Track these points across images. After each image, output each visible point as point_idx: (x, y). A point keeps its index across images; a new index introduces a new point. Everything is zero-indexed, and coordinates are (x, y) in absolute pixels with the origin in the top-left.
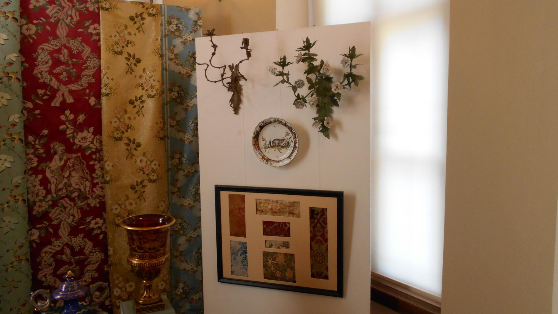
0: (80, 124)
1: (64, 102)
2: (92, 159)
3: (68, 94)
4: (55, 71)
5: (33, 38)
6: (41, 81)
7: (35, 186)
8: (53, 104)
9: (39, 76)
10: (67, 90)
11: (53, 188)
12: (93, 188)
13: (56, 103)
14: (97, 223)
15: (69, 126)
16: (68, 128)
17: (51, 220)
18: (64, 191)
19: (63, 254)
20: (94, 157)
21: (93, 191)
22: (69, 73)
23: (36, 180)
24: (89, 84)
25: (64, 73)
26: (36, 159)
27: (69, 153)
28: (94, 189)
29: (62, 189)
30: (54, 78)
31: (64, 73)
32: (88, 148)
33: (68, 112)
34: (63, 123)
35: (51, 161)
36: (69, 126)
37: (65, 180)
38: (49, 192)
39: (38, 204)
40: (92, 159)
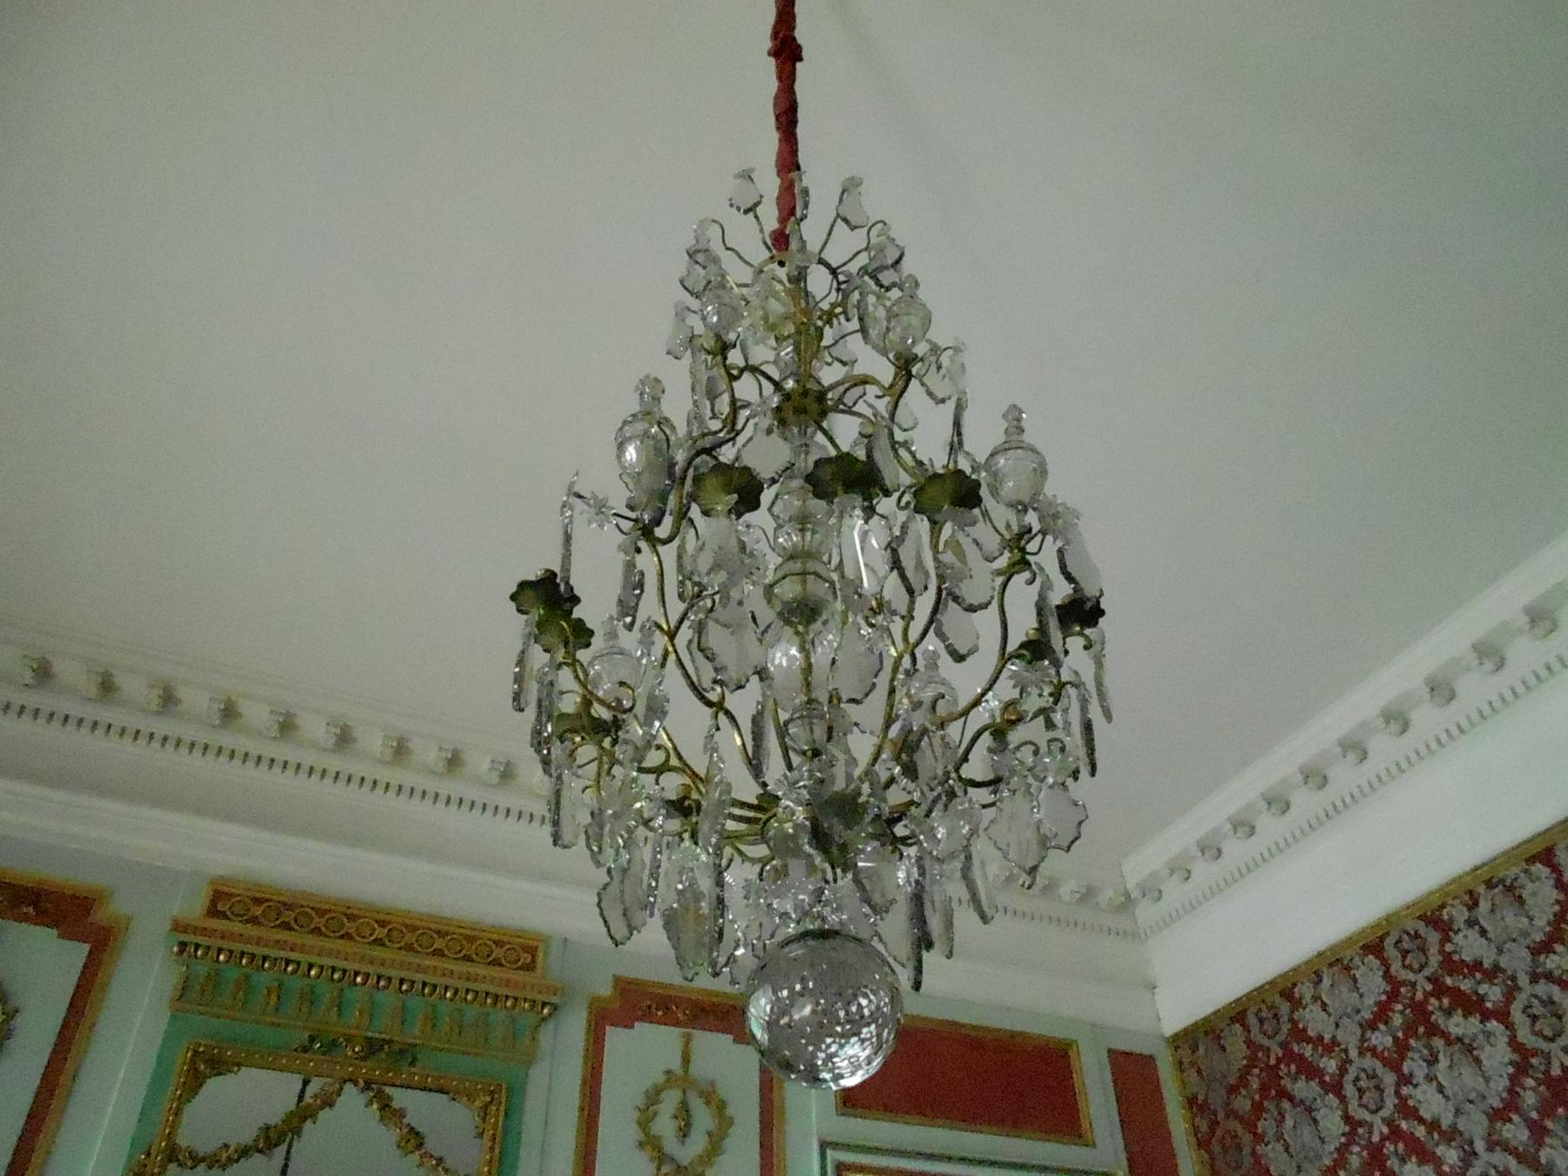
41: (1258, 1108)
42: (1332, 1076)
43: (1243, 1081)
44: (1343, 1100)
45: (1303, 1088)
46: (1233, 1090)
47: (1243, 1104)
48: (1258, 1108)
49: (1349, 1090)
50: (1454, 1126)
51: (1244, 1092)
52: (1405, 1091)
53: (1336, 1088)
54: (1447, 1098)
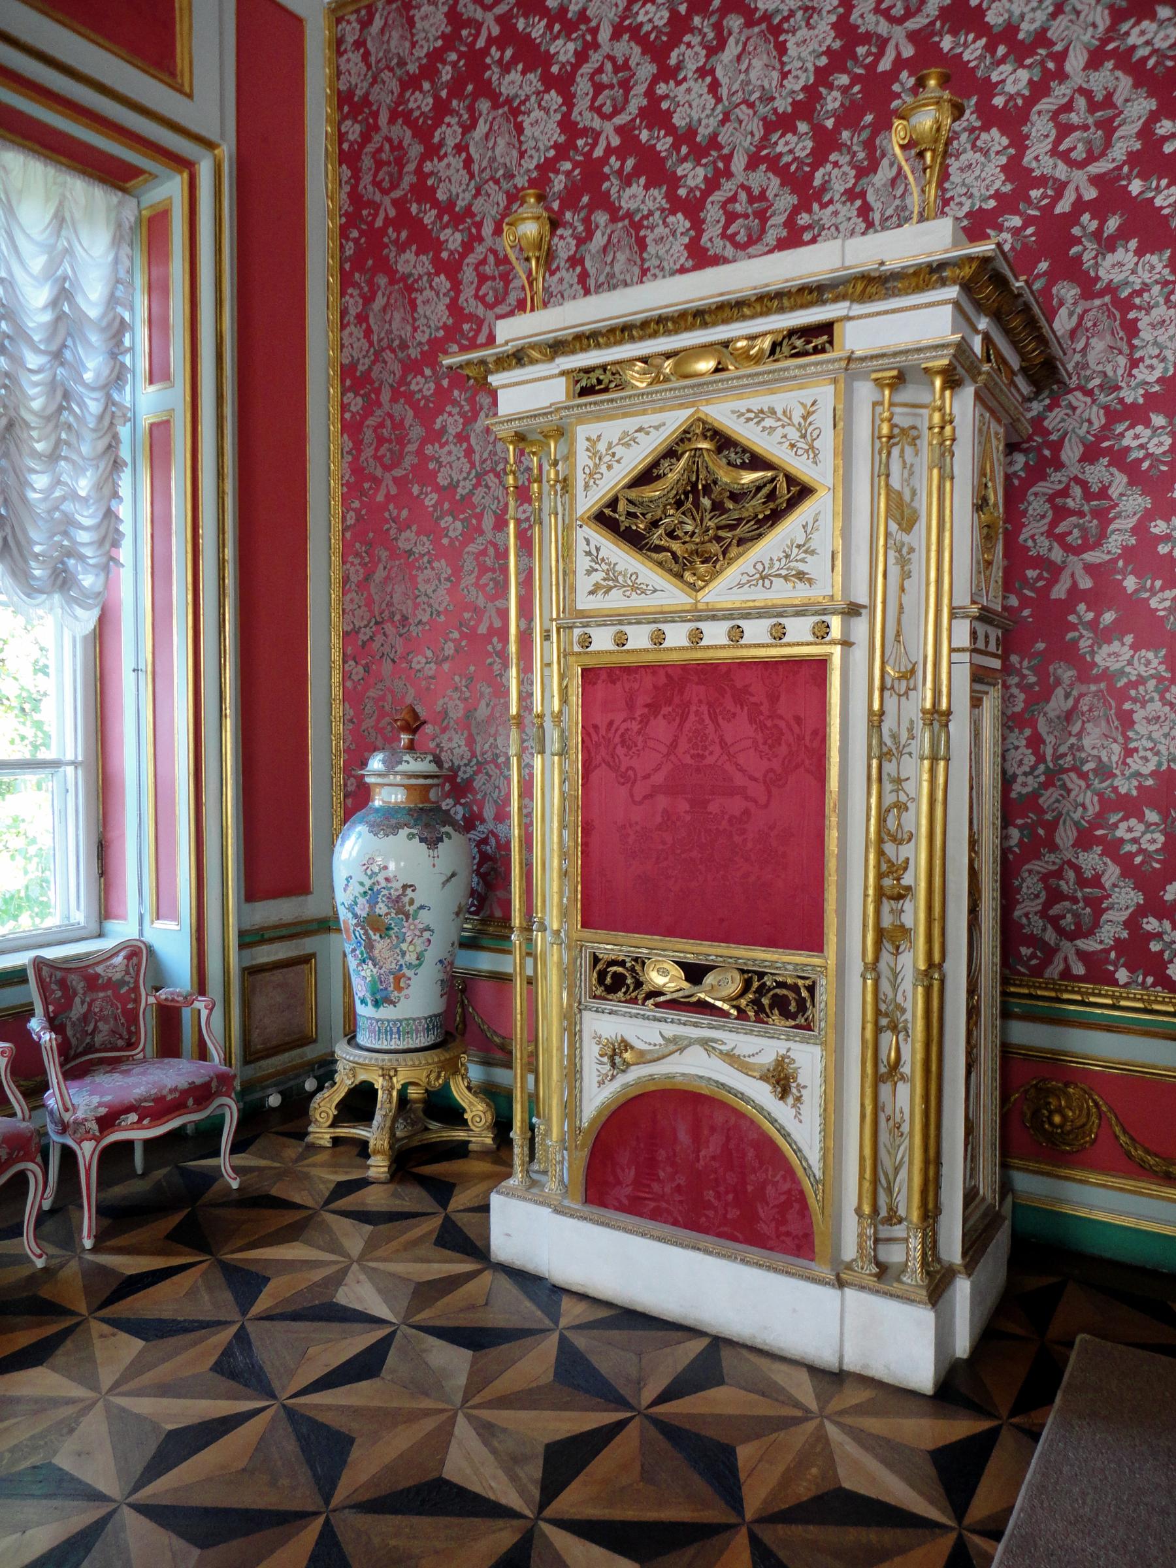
0: (1106, 628)
1: (1074, 589)
2: (1130, 698)
3: (1082, 572)
4: (1057, 531)
5: (1019, 477)
6: (1033, 553)
7: (1017, 748)
8: (1054, 596)
9: (1030, 543)
10: (1081, 565)
11: (1049, 752)
12: (1126, 757)
13: (1059, 592)
14: (1130, 830)
15: (1084, 632)
16: (1082, 636)
17: (1041, 811)
18: (1069, 758)
19: (1061, 877)
20: (1133, 693)
21: (1125, 763)
22: (1084, 530)
23: (1019, 739)
24: (1125, 548)
25: (1075, 531)
26: (1022, 696)
27: (1082, 682)
28: (1129, 760)
29: (1065, 755)
30: (1055, 544)
31: (1075, 531)
32: (1122, 672)
33: (1082, 607)
34: (1074, 627)
35: (1048, 700)
36: (1084, 632)
37: (1073, 740)
38: (1041, 759)
39: (1020, 779)
40: (1130, 698)
41: (441, 109)
42: (452, 253)
43: (429, 71)
44: (456, 286)
45: (516, 83)
46: (411, 83)
47: (421, 102)
48: (441, 109)
49: (468, 275)
50: (713, 138)
51: (426, 86)
52: (661, 89)
53: (451, 269)
54: (719, 100)
